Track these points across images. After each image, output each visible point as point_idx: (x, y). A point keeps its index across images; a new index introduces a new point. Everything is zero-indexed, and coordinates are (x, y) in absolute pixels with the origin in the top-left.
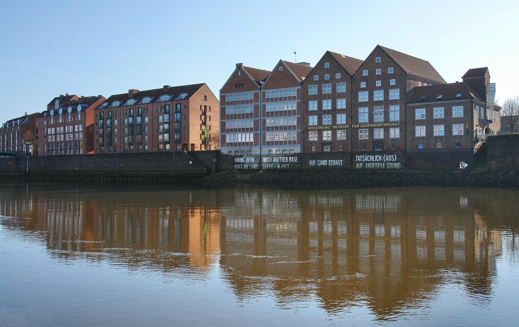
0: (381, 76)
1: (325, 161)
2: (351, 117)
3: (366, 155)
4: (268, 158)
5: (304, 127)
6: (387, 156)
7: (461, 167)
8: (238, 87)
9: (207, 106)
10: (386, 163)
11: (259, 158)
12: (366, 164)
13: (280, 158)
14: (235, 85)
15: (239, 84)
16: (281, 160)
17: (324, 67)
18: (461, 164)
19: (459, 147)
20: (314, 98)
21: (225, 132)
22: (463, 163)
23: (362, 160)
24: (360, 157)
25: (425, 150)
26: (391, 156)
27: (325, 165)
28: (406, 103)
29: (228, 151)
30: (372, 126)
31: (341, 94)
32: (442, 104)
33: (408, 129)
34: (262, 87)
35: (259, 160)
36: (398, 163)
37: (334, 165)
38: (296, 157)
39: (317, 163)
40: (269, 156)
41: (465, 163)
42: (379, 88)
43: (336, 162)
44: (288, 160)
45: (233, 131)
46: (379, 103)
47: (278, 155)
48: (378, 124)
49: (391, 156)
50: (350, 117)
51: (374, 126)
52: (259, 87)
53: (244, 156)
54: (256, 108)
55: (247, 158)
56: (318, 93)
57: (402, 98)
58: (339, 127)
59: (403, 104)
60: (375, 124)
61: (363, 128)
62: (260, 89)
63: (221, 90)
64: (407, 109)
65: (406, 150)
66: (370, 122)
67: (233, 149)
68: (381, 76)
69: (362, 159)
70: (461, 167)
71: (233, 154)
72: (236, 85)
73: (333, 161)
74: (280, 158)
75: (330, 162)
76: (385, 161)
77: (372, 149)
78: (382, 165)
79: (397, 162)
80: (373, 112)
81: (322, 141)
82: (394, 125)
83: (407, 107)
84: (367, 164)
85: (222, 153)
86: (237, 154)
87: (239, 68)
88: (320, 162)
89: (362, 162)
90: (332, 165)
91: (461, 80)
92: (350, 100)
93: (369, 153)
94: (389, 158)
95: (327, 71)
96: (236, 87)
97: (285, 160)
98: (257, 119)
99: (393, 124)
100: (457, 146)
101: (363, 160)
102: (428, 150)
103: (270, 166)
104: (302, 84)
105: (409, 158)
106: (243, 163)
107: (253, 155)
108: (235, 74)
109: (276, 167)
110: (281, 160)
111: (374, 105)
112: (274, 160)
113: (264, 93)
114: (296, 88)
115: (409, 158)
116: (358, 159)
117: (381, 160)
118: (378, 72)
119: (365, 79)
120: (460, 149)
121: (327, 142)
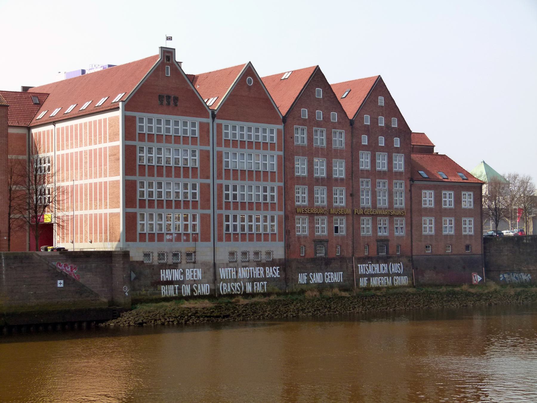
0: (384, 129)
1: (320, 274)
2: (352, 195)
3: (370, 263)
4: (228, 270)
6: (393, 264)
8: (166, 102)
11: (212, 270)
12: (371, 278)
13: (251, 268)
15: (168, 97)
16: (253, 273)
21: (136, 207)
22: (475, 275)
23: (365, 272)
24: (363, 266)
27: (320, 283)
28: (412, 180)
30: (378, 214)
31: (339, 152)
33: (414, 222)
35: (212, 274)
37: (332, 281)
38: (278, 267)
39: (309, 279)
40: (231, 265)
43: (334, 277)
45: (154, 206)
47: (247, 264)
51: (380, 214)
53: (179, 265)
54: (205, 156)
55: (187, 270)
56: (308, 142)
58: (338, 212)
63: (126, 102)
65: (412, 256)
67: (154, 247)
68: (384, 129)
69: (366, 270)
70: (475, 282)
72: (161, 97)
74: (250, 270)
75: (327, 277)
77: (376, 253)
78: (389, 279)
79: (404, 275)
80: (376, 190)
82: (401, 214)
88: (313, 278)
89: (365, 276)
90: (329, 282)
94: (396, 268)
96: (162, 104)
101: (367, 272)
103: (234, 287)
104: (284, 120)
107: (199, 262)
110: (253, 273)
112: (239, 275)
116: (361, 271)
119: (367, 130)
121: (322, 238)
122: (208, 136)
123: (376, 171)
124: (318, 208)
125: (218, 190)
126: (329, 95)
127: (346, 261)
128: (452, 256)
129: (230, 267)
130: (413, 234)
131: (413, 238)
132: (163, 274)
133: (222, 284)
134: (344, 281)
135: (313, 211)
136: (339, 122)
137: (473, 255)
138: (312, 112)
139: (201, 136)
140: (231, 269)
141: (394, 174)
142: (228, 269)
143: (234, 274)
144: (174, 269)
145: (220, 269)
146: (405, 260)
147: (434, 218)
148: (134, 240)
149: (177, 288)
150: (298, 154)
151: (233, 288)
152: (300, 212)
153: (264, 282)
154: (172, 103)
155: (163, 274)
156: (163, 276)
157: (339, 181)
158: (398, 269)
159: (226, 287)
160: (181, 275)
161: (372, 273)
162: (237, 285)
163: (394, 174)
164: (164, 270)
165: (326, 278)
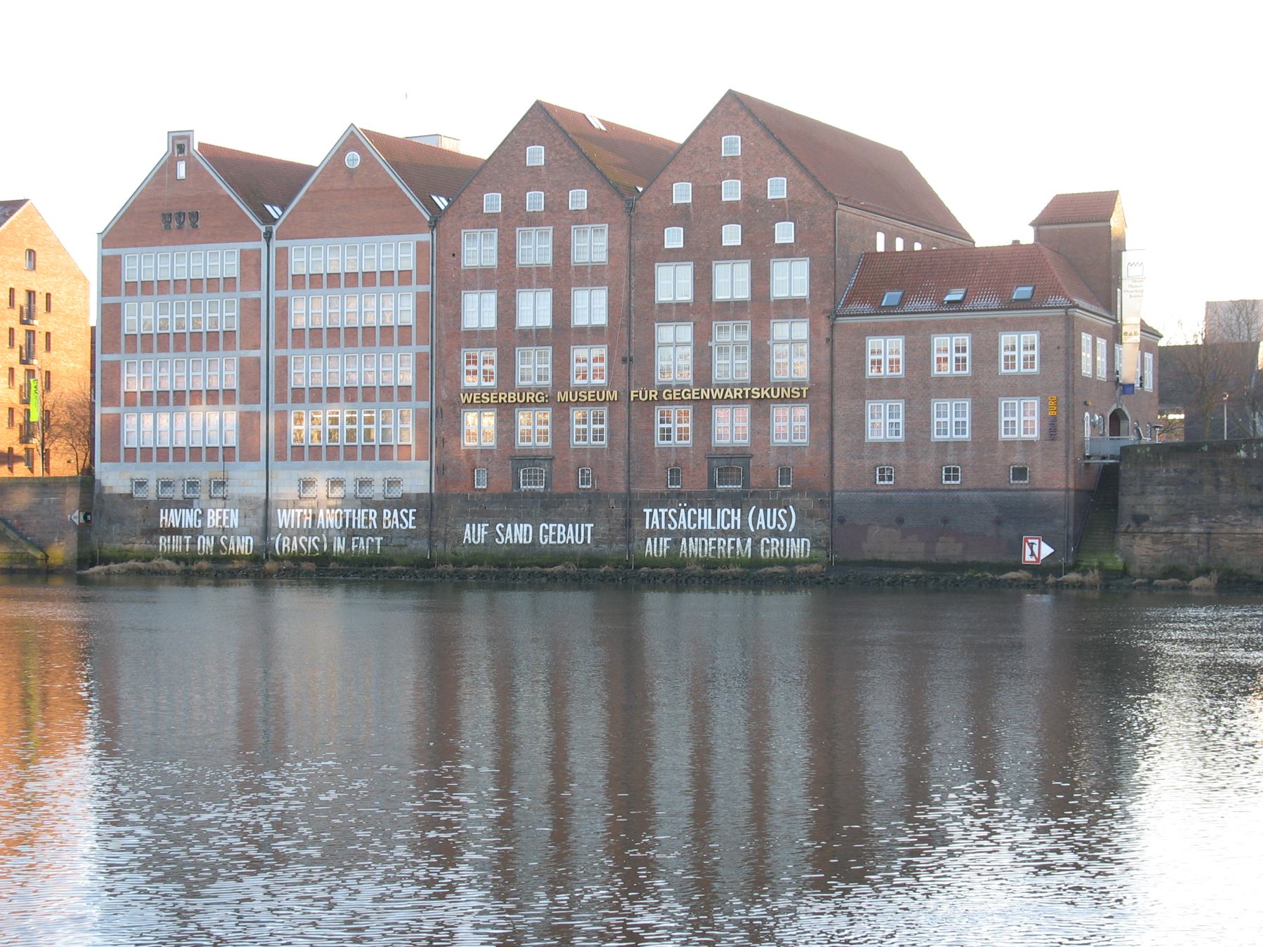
0: (741, 207)
1: (526, 525)
2: (627, 360)
4: (296, 513)
5: (444, 395)
6: (761, 511)
7: (1028, 558)
9: (37, 294)
10: (757, 537)
11: (261, 511)
12: (684, 540)
13: (348, 511)
14: (164, 215)
15: (180, 215)
16: (351, 520)
17: (523, 163)
18: (1029, 544)
19: (1021, 482)
20: (482, 279)
21: (119, 405)
22: (1036, 541)
23: (666, 526)
24: (660, 514)
25: (899, 490)
26: (775, 510)
27: (523, 545)
28: (833, 315)
29: (132, 480)
30: (708, 397)
31: (589, 270)
32: (963, 322)
33: (838, 413)
34: (275, 228)
36: (803, 540)
37: (559, 542)
38: (411, 511)
41: (1042, 543)
42: (733, 254)
43: (566, 533)
44: (380, 519)
45: (152, 401)
46: (732, 310)
48: (729, 390)
49: (775, 510)
50: (624, 360)
51: (714, 397)
52: (263, 229)
53: (195, 501)
54: (250, 310)
55: (209, 511)
57: (819, 293)
58: (579, 397)
59: (823, 317)
60: (717, 390)
61: (672, 402)
62: (268, 236)
63: (103, 235)
64: (835, 338)
65: (832, 493)
66: (698, 380)
67: (152, 473)
68: (741, 207)
69: (668, 520)
71: (151, 493)
72: (167, 218)
73: (555, 529)
74: (344, 514)
75: (546, 532)
76: (752, 530)
77: (705, 484)
78: (744, 544)
79: (798, 534)
80: (710, 344)
81: (514, 450)
82: (788, 396)
83: (835, 328)
84: (688, 542)
85: (102, 488)
86: (168, 493)
87: (181, 149)
88: (504, 533)
89: (666, 533)
90: (551, 542)
91: (1027, 237)
92: (624, 294)
93: (691, 500)
94: (767, 518)
95: (535, 178)
96: (168, 227)
97: (367, 522)
98: (253, 353)
99: (783, 389)
100: (1014, 479)
101: (673, 526)
102: (912, 493)
105: (842, 521)
106: (195, 532)
108: (165, 170)
109: (330, 546)
110: (351, 520)
111: (714, 316)
113: (283, 254)
114: (413, 239)
115: (842, 521)
117: (739, 527)
118: (732, 191)
119: (681, 215)
120: (1027, 490)
121: (534, 453)
122: (259, 273)
123: (712, 302)
124: (522, 391)
125: (277, 367)
126: (564, 156)
127: (609, 501)
128: (960, 494)
129: (300, 508)
130: (836, 441)
131: (835, 450)
132: (164, 515)
133: (281, 537)
134: (596, 542)
135: (504, 399)
136: (591, 209)
137: (1038, 490)
138: (515, 198)
139: (243, 274)
140: (301, 510)
141: (772, 305)
142: (297, 510)
143: (308, 521)
144: (186, 508)
145: (279, 510)
146: (809, 502)
147: (903, 401)
148: (117, 460)
149: (188, 542)
150: (471, 287)
151: (303, 547)
152: (469, 401)
153: (376, 538)
154: (187, 223)
155: (164, 515)
156: (164, 520)
157: (589, 333)
158: (779, 521)
159: (288, 543)
160: (197, 518)
161: (688, 529)
162: (312, 541)
163: (772, 305)
164: (167, 510)
165: (544, 534)
